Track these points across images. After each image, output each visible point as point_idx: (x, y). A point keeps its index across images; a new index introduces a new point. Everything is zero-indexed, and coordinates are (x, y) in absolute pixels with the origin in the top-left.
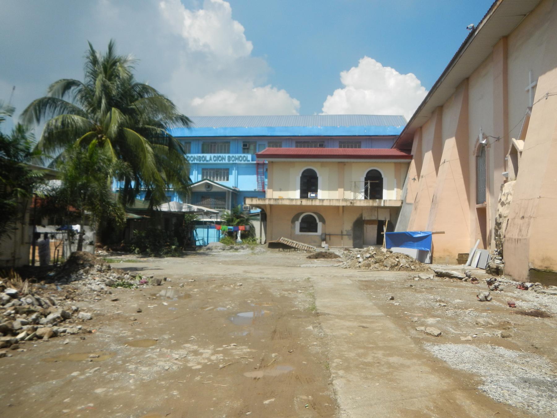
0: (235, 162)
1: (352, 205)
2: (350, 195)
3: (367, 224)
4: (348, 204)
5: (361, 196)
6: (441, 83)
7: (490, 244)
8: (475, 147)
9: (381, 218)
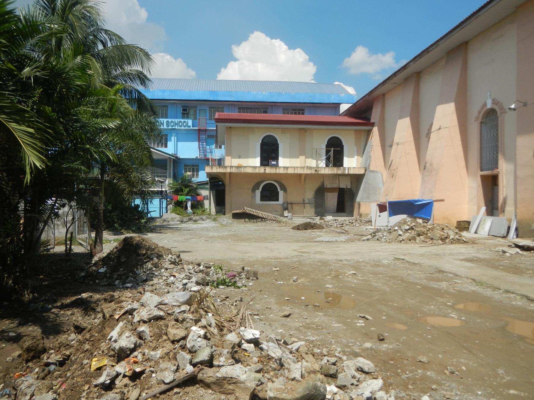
0: (174, 128)
1: (316, 173)
2: (312, 163)
3: (327, 192)
4: (313, 172)
5: (322, 164)
6: (436, 47)
7: (504, 211)
8: (479, 113)
9: (342, 186)
